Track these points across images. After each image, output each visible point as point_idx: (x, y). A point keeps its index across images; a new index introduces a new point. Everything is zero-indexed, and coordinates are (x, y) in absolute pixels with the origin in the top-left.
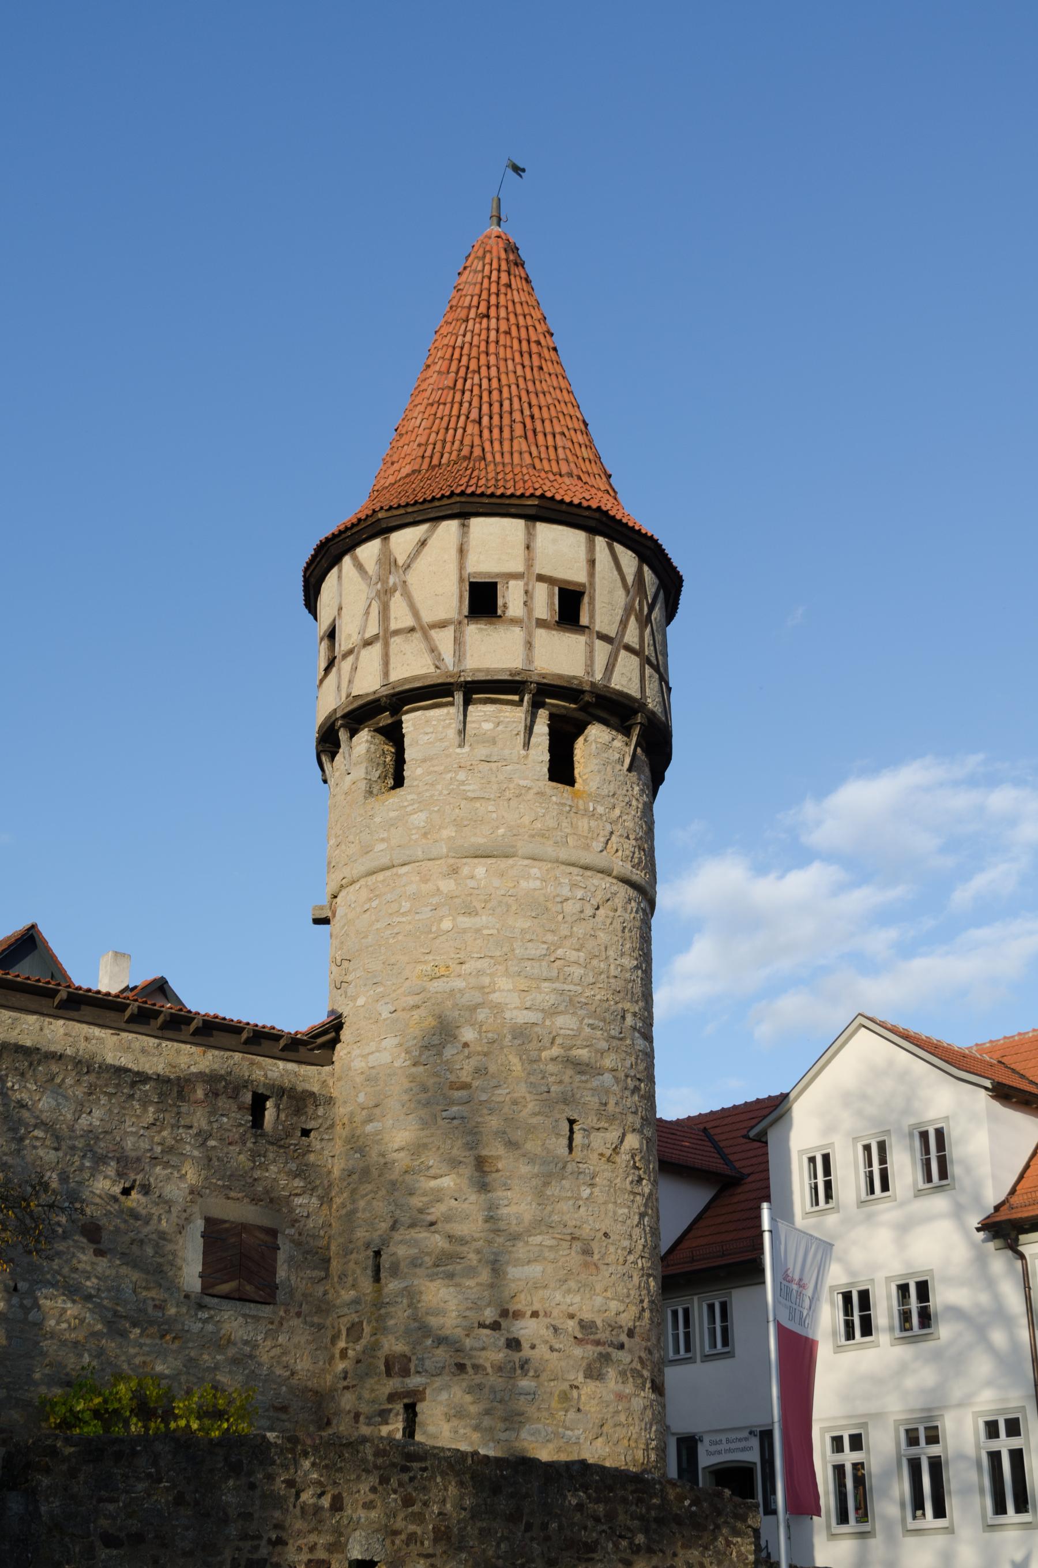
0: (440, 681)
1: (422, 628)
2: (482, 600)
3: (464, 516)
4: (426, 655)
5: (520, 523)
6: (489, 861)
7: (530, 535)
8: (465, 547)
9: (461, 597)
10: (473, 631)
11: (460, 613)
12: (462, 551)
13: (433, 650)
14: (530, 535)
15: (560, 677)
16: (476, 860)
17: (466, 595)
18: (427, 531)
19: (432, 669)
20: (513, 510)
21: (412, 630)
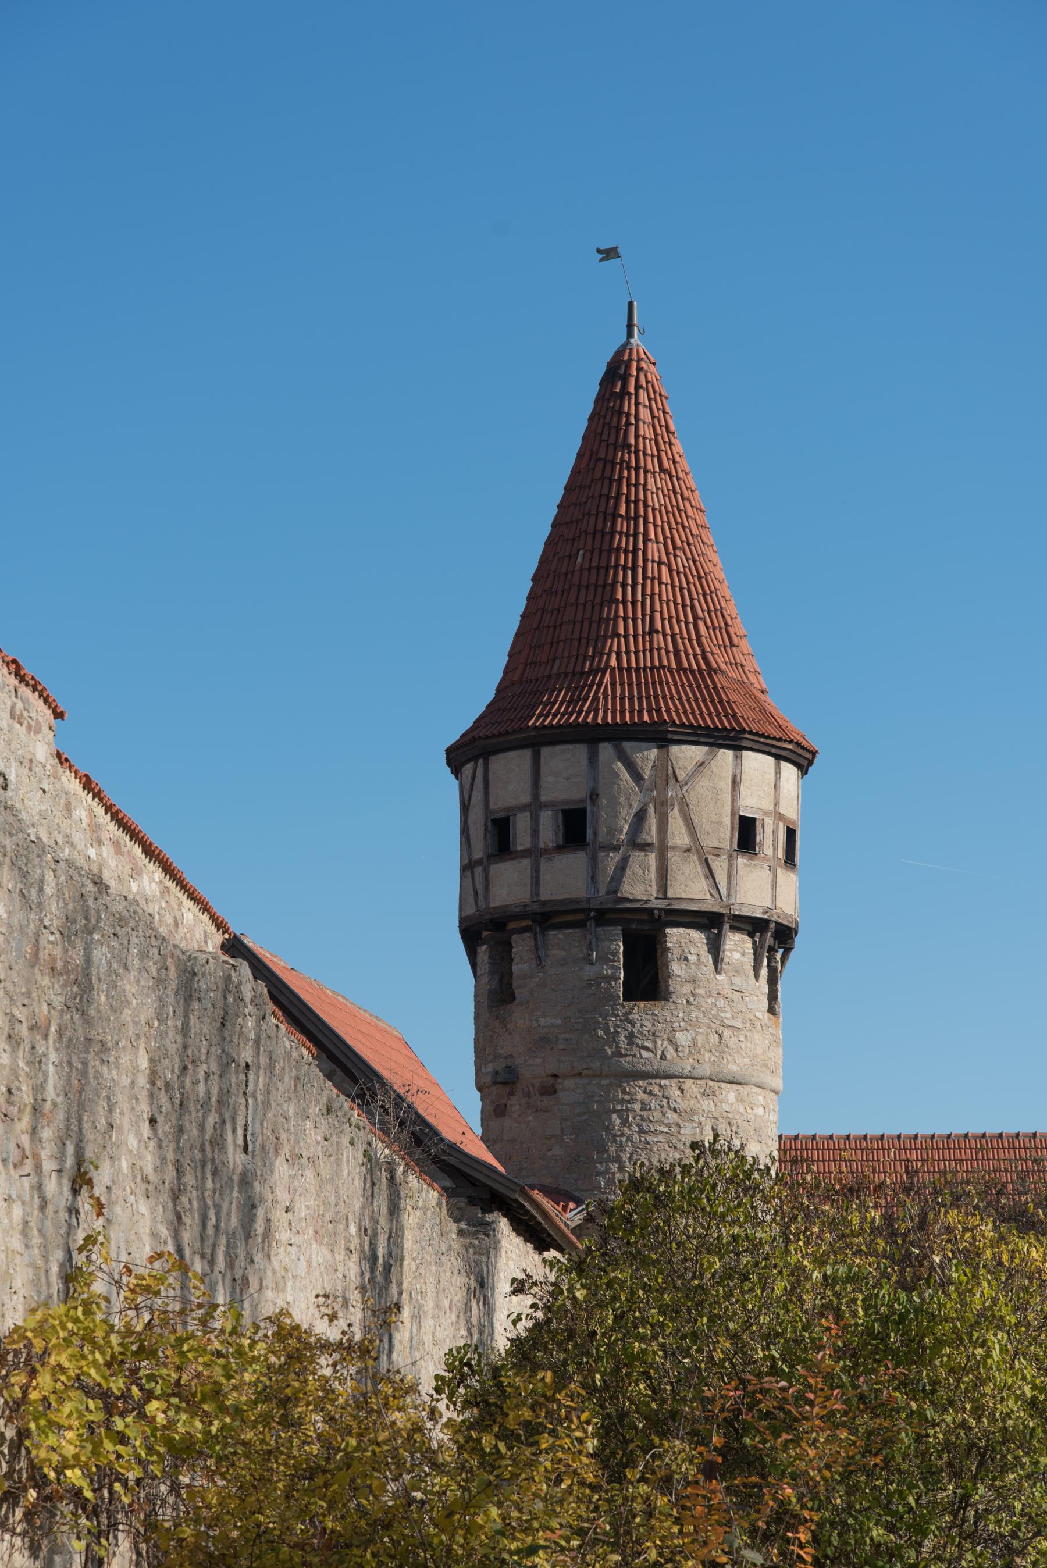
0: (714, 910)
1: (698, 851)
2: (746, 833)
3: (738, 748)
4: (703, 880)
5: (771, 759)
6: (739, 1087)
7: (778, 771)
8: (738, 779)
9: (733, 828)
10: (741, 861)
11: (731, 845)
12: (735, 783)
13: (711, 874)
14: (778, 771)
15: (786, 915)
16: (729, 1086)
17: (737, 826)
18: (707, 754)
19: (709, 897)
20: (774, 750)
21: (688, 850)
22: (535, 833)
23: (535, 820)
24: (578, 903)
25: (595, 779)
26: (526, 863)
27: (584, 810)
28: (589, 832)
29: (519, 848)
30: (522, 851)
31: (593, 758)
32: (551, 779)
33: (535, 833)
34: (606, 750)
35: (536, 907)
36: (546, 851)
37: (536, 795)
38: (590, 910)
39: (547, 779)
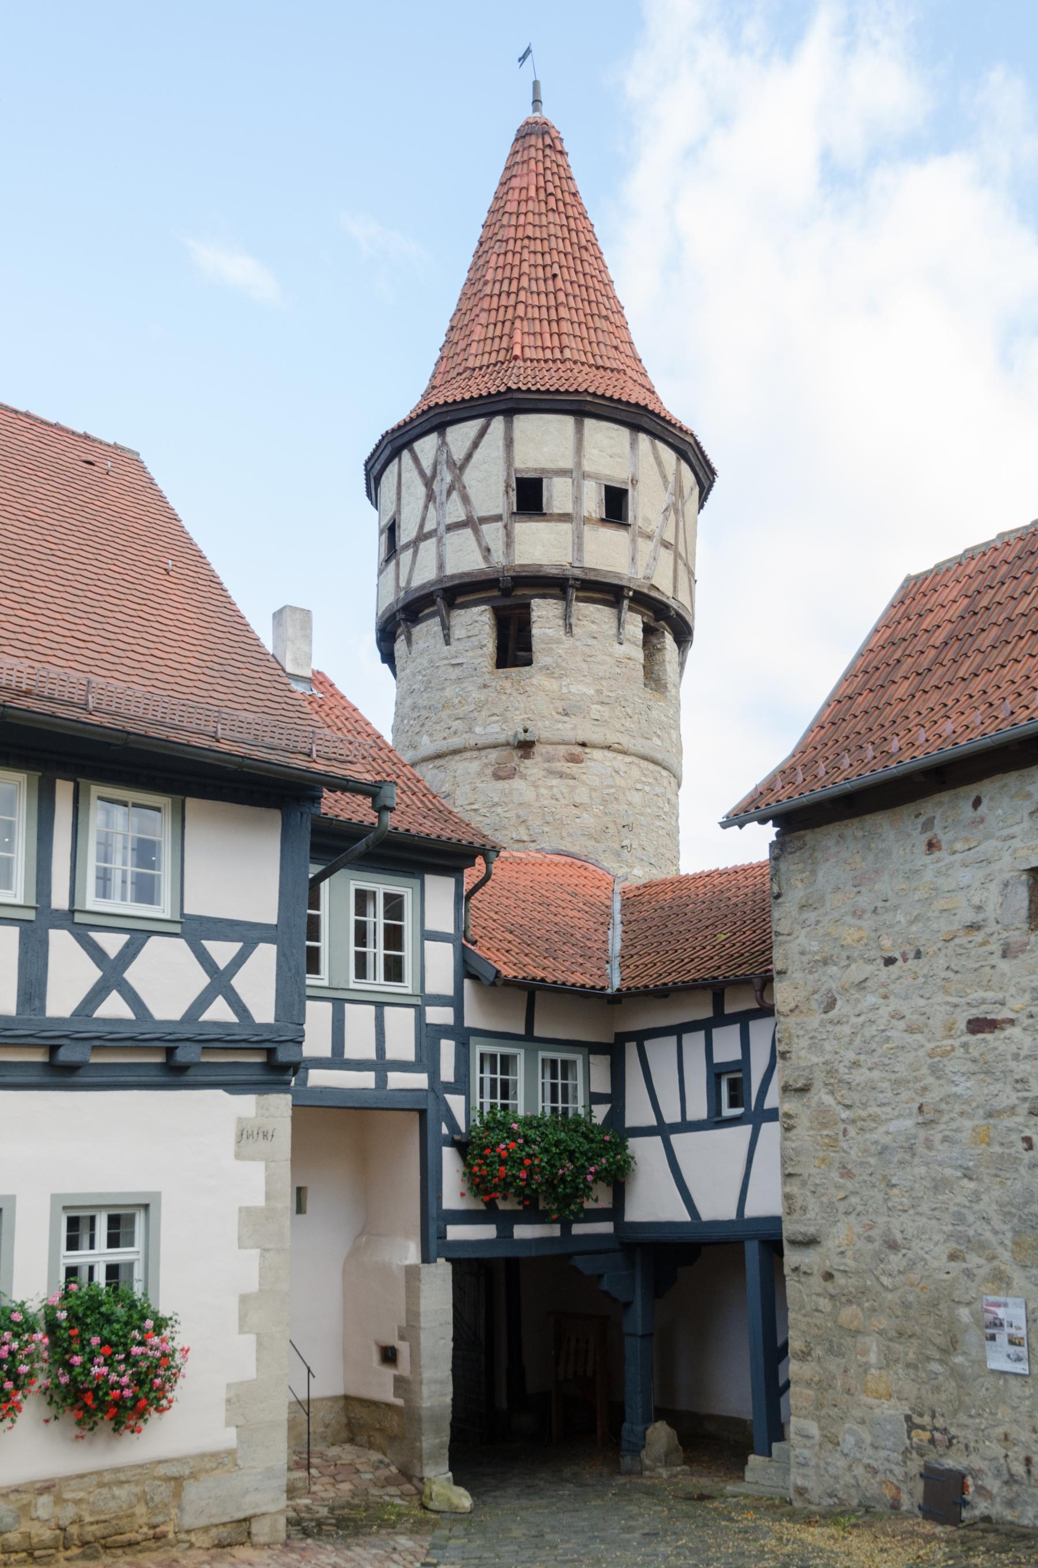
22: (577, 499)
23: (578, 489)
24: (621, 579)
25: (635, 465)
26: (566, 527)
27: (626, 491)
28: (630, 514)
29: (556, 511)
30: (560, 515)
31: (634, 444)
32: (595, 452)
33: (577, 499)
34: (643, 439)
35: (578, 573)
36: (587, 520)
37: (579, 464)
38: (630, 589)
39: (591, 451)
